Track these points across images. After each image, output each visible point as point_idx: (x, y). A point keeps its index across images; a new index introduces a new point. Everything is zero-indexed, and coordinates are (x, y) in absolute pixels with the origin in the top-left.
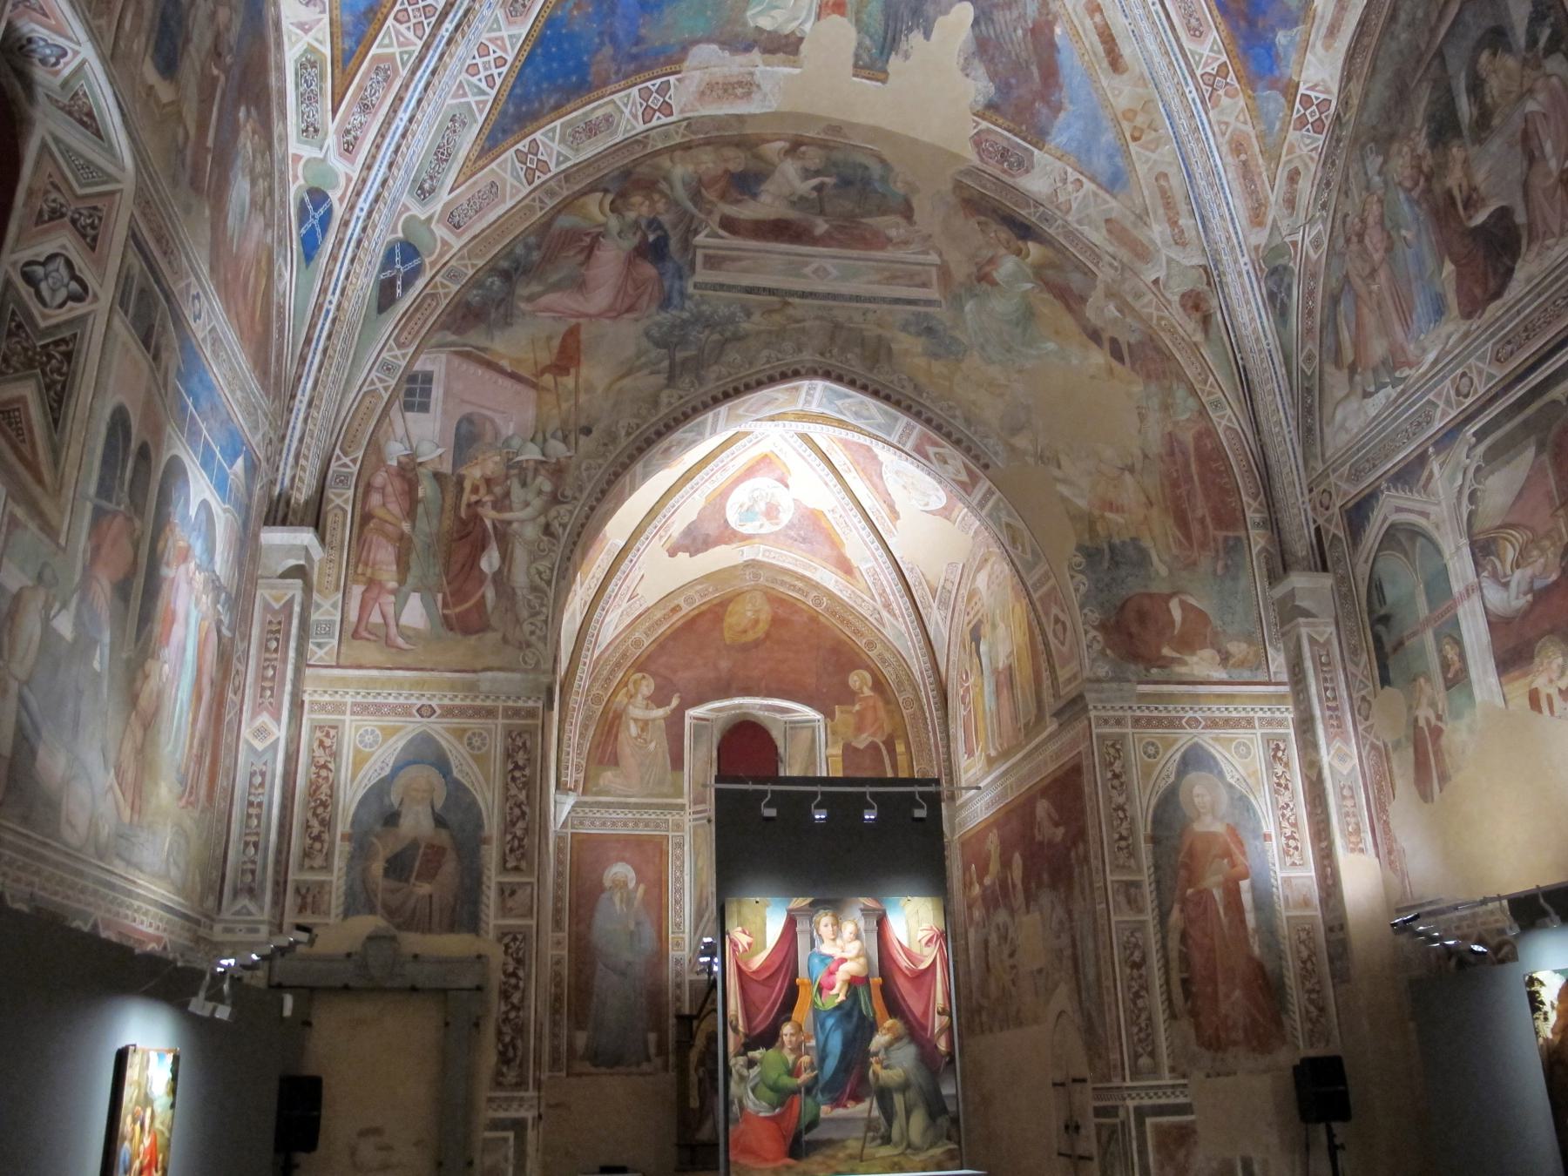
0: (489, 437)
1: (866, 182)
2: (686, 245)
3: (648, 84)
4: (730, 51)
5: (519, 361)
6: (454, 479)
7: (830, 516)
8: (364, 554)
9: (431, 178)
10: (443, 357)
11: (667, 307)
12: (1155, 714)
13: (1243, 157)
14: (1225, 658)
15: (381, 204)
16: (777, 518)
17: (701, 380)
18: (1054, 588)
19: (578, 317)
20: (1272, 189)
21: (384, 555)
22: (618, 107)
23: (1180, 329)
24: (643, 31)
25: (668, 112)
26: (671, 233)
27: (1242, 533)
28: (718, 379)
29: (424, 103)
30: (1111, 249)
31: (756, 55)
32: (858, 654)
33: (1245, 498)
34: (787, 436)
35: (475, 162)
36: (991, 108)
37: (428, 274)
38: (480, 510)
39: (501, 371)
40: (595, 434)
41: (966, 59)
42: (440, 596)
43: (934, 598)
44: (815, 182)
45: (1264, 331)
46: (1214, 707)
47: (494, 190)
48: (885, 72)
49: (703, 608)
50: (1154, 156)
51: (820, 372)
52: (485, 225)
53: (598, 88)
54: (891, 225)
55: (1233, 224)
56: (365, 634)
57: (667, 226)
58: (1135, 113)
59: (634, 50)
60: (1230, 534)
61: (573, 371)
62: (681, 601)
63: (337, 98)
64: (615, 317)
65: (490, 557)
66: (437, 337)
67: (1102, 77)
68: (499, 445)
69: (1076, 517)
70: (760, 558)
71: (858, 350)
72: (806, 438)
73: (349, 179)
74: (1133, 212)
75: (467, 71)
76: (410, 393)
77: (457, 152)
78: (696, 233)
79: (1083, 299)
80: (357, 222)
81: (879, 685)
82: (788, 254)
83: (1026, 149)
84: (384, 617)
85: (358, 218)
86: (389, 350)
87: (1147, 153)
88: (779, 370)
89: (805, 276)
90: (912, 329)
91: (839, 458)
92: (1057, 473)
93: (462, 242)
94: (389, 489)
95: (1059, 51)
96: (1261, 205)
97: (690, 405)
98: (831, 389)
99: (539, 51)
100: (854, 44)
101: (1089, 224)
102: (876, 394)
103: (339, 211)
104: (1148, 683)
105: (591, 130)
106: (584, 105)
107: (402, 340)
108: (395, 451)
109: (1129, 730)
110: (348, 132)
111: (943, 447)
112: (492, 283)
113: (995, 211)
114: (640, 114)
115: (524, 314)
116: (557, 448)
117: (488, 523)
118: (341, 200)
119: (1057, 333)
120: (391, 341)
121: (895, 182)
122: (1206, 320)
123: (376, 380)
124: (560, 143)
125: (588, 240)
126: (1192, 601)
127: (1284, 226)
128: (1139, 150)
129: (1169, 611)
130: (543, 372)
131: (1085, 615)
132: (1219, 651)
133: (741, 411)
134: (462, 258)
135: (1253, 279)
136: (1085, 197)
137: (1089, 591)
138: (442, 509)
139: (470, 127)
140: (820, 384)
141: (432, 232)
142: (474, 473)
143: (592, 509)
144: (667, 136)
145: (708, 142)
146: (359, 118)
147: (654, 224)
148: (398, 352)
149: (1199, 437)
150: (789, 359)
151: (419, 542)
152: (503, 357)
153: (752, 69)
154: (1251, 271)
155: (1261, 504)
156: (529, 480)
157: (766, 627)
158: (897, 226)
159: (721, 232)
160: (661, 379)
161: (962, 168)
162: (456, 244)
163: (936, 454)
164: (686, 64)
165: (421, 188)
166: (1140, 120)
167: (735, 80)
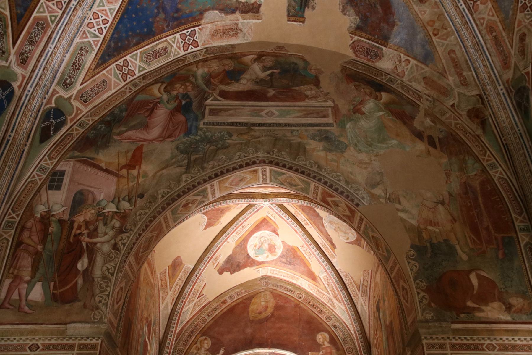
0: (90, 201)
2: (201, 106)
3: (185, 32)
4: (224, 13)
5: (110, 163)
6: (69, 222)
7: (301, 249)
8: (15, 262)
9: (70, 78)
10: (72, 163)
11: (189, 134)
12: (465, 341)
13: (494, 34)
14: (509, 308)
15: (38, 88)
16: (274, 252)
17: (203, 169)
18: (399, 269)
19: (142, 141)
20: (512, 48)
21: (26, 262)
22: (170, 44)
23: (468, 128)
25: (197, 45)
26: (193, 100)
27: (515, 235)
28: (213, 168)
29: (61, 39)
30: (427, 92)
32: (321, 324)
33: (513, 215)
34: (272, 207)
35: (94, 70)
36: (358, 29)
37: (69, 125)
38: (81, 237)
39: (100, 168)
40: (146, 197)
41: (343, 6)
42: (52, 283)
43: (359, 291)
45: (516, 124)
46: (504, 338)
47: (105, 84)
48: (304, 17)
49: (239, 301)
50: (446, 42)
51: (267, 162)
52: (100, 101)
54: (308, 90)
55: (492, 70)
56: (7, 306)
57: (192, 97)
58: (434, 22)
59: (176, 15)
60: (506, 235)
61: (137, 167)
62: (227, 298)
63: (15, 37)
64: (162, 141)
65: (83, 262)
66: (70, 154)
67: (414, 6)
68: (95, 205)
69: (409, 229)
70: (269, 274)
71: (288, 150)
72: (281, 206)
73: (24, 77)
74: (438, 72)
75: (87, 26)
76: (52, 181)
77: (84, 66)
78: (207, 99)
79: (412, 118)
80: (26, 97)
81: (333, 340)
82: (253, 106)
83: (379, 48)
84: (20, 295)
85: (27, 95)
86: (44, 161)
87: (443, 41)
88: (245, 162)
89: (261, 116)
90: (318, 138)
91: (302, 217)
92: (398, 206)
93: (88, 110)
94: (34, 229)
96: (507, 57)
97: (197, 181)
99: (126, 16)
101: (415, 82)
102: (297, 170)
103: (17, 92)
104: (458, 323)
105: (156, 55)
107: (52, 156)
108: (41, 209)
109: (449, 352)
110: (22, 54)
111: (334, 197)
112: (101, 127)
114: (181, 46)
115: (115, 141)
116: (125, 205)
117: (84, 244)
118: (19, 87)
119: (398, 135)
120: (46, 157)
121: (311, 70)
122: (483, 124)
123: (36, 176)
124: (140, 61)
125: (152, 105)
126: (484, 274)
127: (521, 66)
128: (437, 40)
129: (469, 280)
130: (121, 169)
131: (417, 284)
132: (504, 303)
133: (227, 184)
134: (88, 116)
135: (507, 96)
136: (411, 68)
137: (419, 270)
138: (61, 237)
139: (91, 53)
141: (72, 105)
142: (80, 219)
143: (140, 235)
144: (195, 56)
145: (216, 58)
146: (28, 48)
147: (186, 96)
148: (49, 162)
149: (482, 184)
150: (251, 156)
151: (45, 256)
152: (101, 161)
153: (237, 22)
154: (505, 93)
155: (524, 218)
156: (108, 222)
157: (272, 310)
158: (311, 90)
159: (219, 98)
160: (183, 169)
162: (85, 110)
163: (332, 201)
164: (203, 22)
165: (65, 82)
166: (437, 25)
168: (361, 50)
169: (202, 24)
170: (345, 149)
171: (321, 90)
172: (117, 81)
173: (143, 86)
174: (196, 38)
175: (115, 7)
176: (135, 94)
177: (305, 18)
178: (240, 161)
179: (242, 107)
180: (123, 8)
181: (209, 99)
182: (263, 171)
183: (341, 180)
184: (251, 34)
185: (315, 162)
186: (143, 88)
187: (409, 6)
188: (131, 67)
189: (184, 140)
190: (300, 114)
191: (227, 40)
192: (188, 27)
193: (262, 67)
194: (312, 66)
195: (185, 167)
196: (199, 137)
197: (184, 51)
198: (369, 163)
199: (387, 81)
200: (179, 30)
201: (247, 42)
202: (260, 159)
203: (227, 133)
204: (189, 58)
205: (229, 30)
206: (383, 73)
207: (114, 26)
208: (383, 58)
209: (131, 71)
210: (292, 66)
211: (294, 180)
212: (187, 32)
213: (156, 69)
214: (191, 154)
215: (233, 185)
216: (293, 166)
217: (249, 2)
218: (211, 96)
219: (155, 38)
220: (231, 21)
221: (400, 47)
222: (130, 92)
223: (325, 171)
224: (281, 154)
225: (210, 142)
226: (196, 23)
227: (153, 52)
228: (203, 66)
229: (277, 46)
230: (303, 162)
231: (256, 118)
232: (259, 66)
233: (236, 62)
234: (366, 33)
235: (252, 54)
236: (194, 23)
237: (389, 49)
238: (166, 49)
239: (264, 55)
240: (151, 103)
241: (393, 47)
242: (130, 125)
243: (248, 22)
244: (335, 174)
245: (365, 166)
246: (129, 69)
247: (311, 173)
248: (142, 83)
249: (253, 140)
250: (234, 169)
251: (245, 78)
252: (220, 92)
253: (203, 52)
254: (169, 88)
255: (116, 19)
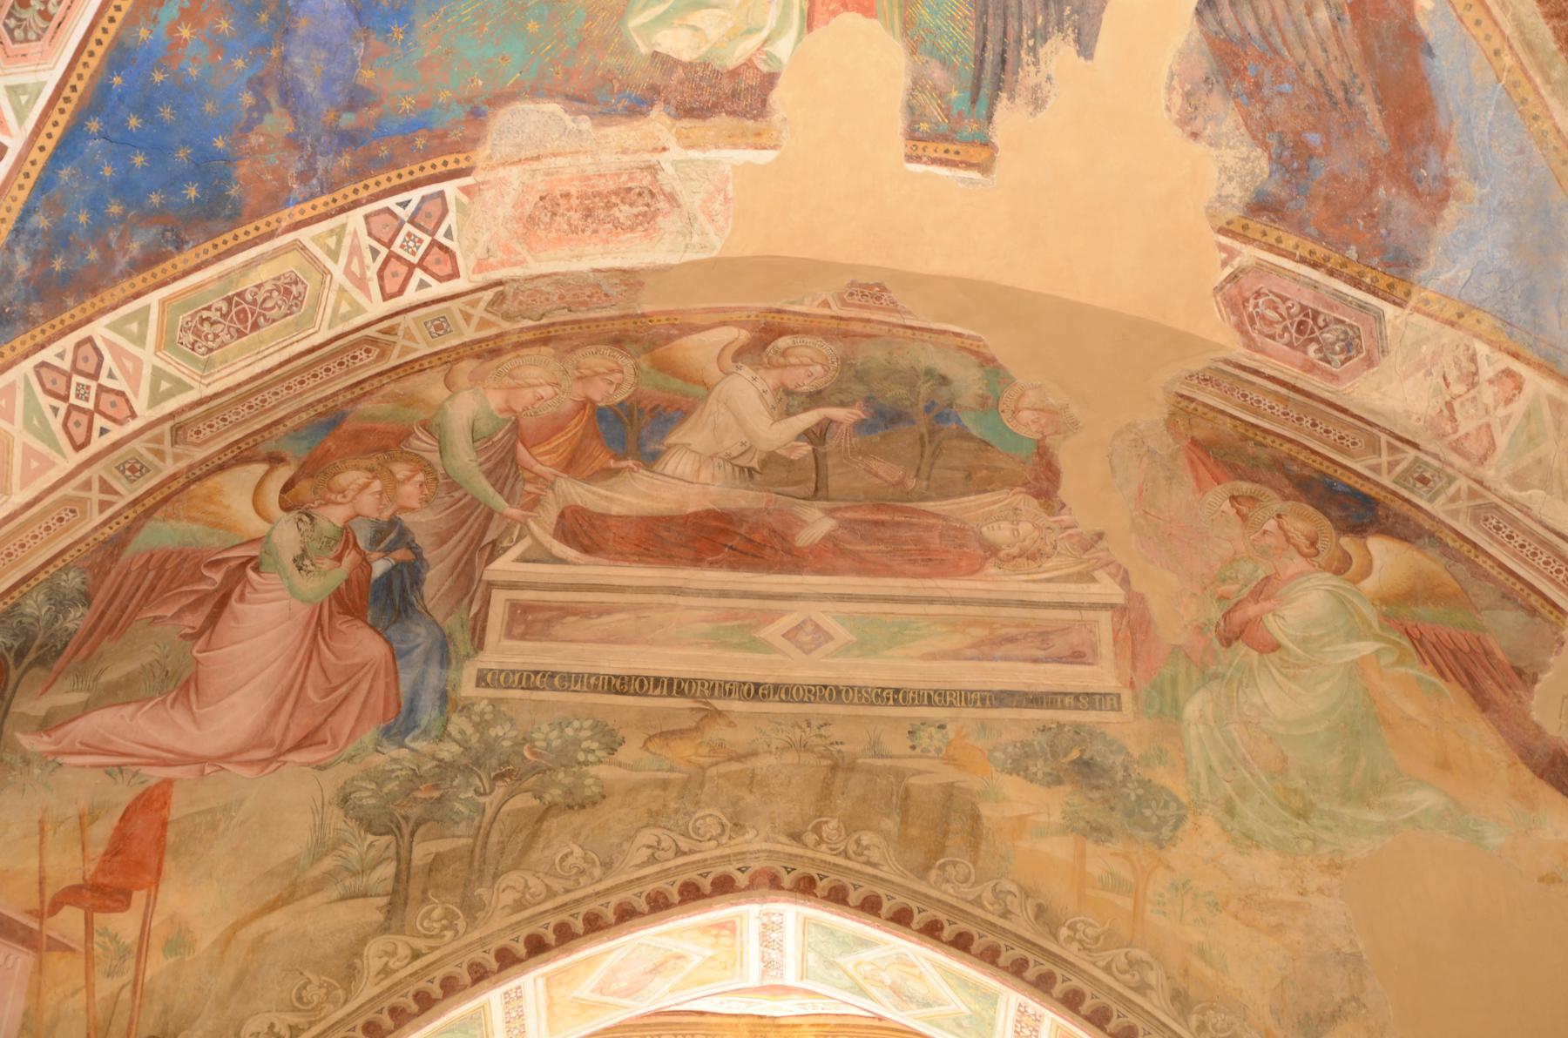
1: (941, 414)
2: (467, 581)
3: (390, 202)
4: (592, 115)
17: (471, 908)
19: (166, 764)
22: (314, 260)
24: (367, 76)
25: (448, 270)
28: (519, 906)
31: (659, 123)
41: (1187, 96)
44: (809, 418)
48: (986, 144)
51: (787, 880)
53: (257, 214)
57: (422, 540)
59: (348, 120)
61: (139, 897)
64: (268, 761)
67: (1553, 103)
71: (890, 825)
78: (495, 551)
79: (1524, 676)
82: (723, 594)
83: (1363, 307)
89: (765, 647)
90: (1039, 767)
95: (1429, 51)
97: (439, 974)
98: (821, 927)
99: (94, 126)
100: (903, 83)
101: (1545, 485)
102: (931, 931)
106: (219, 258)
113: (1278, 465)
114: (372, 274)
115: (27, 762)
121: (1016, 411)
124: (158, 348)
125: (217, 576)
130: (56, 907)
133: (585, 989)
136: (1528, 415)
140: (791, 913)
145: (544, 338)
147: (391, 533)
150: (710, 850)
159: (559, 549)
160: (370, 912)
161: (1197, 366)
164: (481, 154)
167: (612, 186)
168: (1271, 314)
169: (480, 164)
170: (1176, 828)
171: (1065, 518)
172: (38, 445)
173: (174, 477)
174: (448, 234)
175: (42, 77)
176: (132, 515)
177: (994, 148)
178: (658, 876)
179: (672, 599)
180: (81, 86)
181: (506, 550)
182: (764, 925)
183: (1152, 989)
184: (721, 221)
185: (1021, 888)
186: (175, 486)
187: (1524, 101)
188: (111, 375)
189: (378, 760)
190: (955, 641)
191: (599, 248)
192: (407, 179)
193: (776, 390)
194: (1022, 395)
195: (383, 901)
196: (456, 749)
197: (386, 297)
198: (1295, 906)
199: (1401, 479)
200: (364, 194)
201: (703, 256)
202: (756, 865)
203: (594, 726)
204: (408, 335)
205: (614, 199)
206: (1384, 438)
207: (35, 172)
208: (1385, 362)
209: (113, 397)
210: (924, 389)
211: (920, 977)
212: (404, 205)
213: (239, 385)
214: (412, 834)
215: (615, 994)
216: (913, 905)
217: (717, 64)
218: (520, 537)
219: (240, 231)
220: (624, 152)
221: (1471, 307)
222: (104, 505)
223: (1070, 939)
224: (858, 842)
225: (508, 774)
226: (450, 159)
227: (229, 300)
228: (476, 379)
229: (852, 284)
230: (964, 888)
231: (737, 655)
232: (760, 385)
233: (644, 362)
234: (1305, 236)
235: (724, 324)
236: (438, 161)
237: (1416, 318)
238: (294, 290)
239: (782, 333)
240: (215, 564)
241: (1434, 308)
242: (104, 679)
243: (708, 162)
244: (1119, 957)
245: (1274, 920)
246: (102, 389)
247: (1002, 943)
248: (169, 460)
249: (724, 768)
250: (626, 914)
251: (686, 446)
252: (562, 516)
253: (482, 305)
254: (304, 486)
255: (42, 140)
